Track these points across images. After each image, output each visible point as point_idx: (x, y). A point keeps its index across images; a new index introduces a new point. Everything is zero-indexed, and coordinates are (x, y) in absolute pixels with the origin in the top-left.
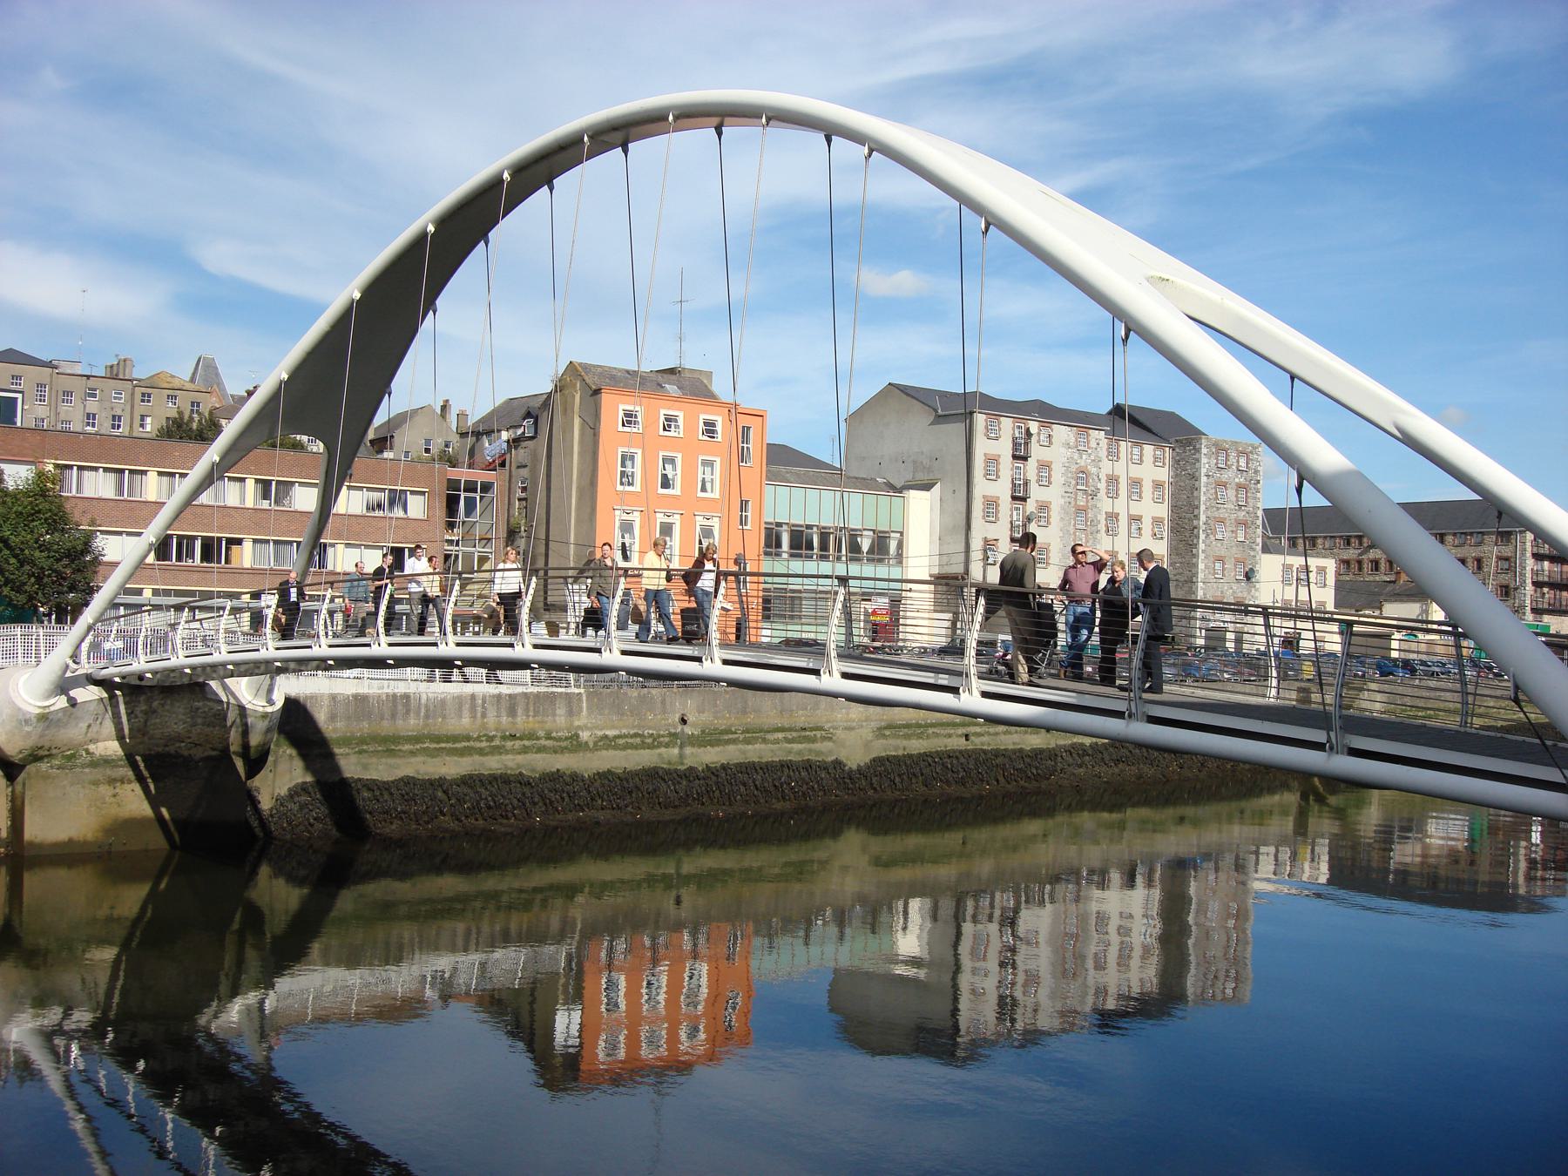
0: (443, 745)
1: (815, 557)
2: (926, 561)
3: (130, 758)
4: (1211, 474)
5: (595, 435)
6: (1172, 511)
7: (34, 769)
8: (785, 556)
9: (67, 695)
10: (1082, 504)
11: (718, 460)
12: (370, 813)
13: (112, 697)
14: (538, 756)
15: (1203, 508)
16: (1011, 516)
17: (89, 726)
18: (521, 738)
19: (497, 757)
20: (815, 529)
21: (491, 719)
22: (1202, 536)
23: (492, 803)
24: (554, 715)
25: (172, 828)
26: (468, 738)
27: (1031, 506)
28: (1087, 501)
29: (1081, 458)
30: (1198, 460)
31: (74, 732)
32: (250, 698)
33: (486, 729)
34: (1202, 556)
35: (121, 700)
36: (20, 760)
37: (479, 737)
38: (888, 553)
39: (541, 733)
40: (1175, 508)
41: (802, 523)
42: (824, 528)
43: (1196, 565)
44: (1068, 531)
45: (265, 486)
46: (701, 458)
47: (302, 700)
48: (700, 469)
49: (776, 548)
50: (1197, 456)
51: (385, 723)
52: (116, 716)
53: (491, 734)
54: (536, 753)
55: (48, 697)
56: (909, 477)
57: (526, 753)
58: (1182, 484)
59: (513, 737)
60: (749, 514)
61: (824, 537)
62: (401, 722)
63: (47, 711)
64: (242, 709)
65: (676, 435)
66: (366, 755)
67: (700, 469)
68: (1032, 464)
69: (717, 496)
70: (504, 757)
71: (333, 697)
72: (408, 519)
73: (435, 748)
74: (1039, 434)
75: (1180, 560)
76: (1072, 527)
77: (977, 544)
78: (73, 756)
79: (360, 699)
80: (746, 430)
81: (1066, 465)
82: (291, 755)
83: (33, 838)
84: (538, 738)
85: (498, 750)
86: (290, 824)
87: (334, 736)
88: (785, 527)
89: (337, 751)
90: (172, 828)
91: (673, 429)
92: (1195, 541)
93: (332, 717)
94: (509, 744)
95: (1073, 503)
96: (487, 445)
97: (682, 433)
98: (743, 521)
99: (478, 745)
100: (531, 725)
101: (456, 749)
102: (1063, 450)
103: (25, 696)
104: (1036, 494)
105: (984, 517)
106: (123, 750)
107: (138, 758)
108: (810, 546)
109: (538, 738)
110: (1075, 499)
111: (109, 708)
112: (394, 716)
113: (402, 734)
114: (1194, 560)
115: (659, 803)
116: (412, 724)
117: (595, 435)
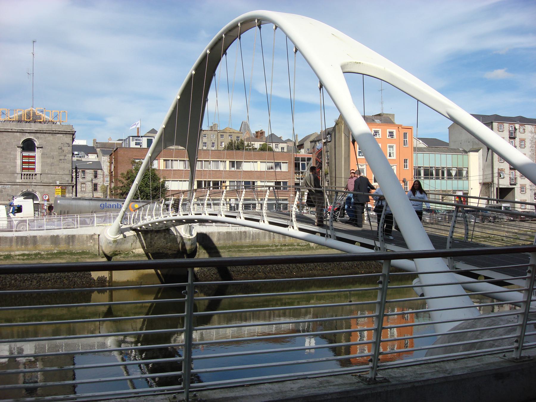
0: (259, 248)
1: (434, 178)
2: (478, 178)
3: (147, 254)
7: (115, 258)
8: (422, 178)
9: (123, 234)
11: (395, 145)
12: (233, 272)
13: (138, 235)
14: (295, 252)
17: (132, 244)
18: (288, 246)
19: (279, 252)
20: (434, 168)
23: (277, 268)
25: (162, 276)
26: (268, 246)
31: (127, 246)
32: (184, 234)
33: (274, 243)
35: (141, 235)
36: (110, 255)
37: (272, 245)
39: (295, 244)
41: (428, 166)
42: (437, 168)
45: (233, 164)
46: (388, 145)
47: (208, 234)
48: (388, 149)
51: (238, 241)
52: (141, 241)
53: (277, 245)
54: (294, 251)
55: (117, 234)
56: (471, 147)
57: (290, 251)
59: (285, 245)
60: (408, 164)
61: (437, 171)
62: (243, 241)
63: (116, 239)
64: (181, 237)
65: (379, 137)
66: (231, 252)
67: (388, 149)
68: (517, 140)
69: (395, 158)
70: (282, 252)
71: (219, 233)
72: (282, 172)
73: (256, 250)
74: (519, 129)
77: (496, 171)
78: (128, 254)
79: (229, 234)
80: (405, 134)
81: (531, 140)
82: (204, 253)
83: (115, 280)
84: (294, 246)
85: (280, 250)
86: (204, 275)
87: (220, 246)
88: (422, 168)
89: (220, 251)
90: (162, 276)
91: (377, 135)
93: (219, 240)
94: (283, 248)
96: (318, 145)
97: (381, 137)
98: (405, 166)
99: (272, 248)
100: (291, 241)
101: (264, 250)
102: (530, 134)
103: (109, 235)
105: (498, 161)
106: (144, 252)
107: (150, 254)
108: (432, 175)
109: (294, 246)
111: (137, 238)
112: (241, 239)
113: (244, 245)
115: (342, 268)
116: (248, 241)
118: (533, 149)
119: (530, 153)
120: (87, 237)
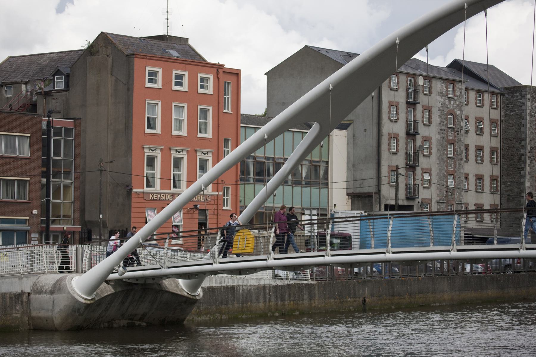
2: (344, 185)
4: (533, 114)
5: (128, 89)
6: (503, 142)
8: (252, 181)
10: (451, 138)
11: (211, 109)
15: (528, 139)
16: (406, 148)
21: (273, 303)
22: (528, 162)
24: (303, 299)
27: (419, 140)
28: (455, 137)
29: (450, 103)
30: (524, 104)
34: (528, 177)
38: (319, 178)
40: (504, 140)
43: (523, 184)
44: (443, 159)
49: (246, 175)
50: (523, 100)
58: (511, 122)
68: (419, 108)
75: (511, 180)
76: (445, 156)
81: (441, 109)
92: (523, 165)
95: (445, 138)
102: (438, 98)
104: (423, 131)
110: (447, 135)
112: (227, 303)
114: (522, 180)
117: (128, 89)
118: (443, 128)
119: (438, 137)
120: (11, 298)
